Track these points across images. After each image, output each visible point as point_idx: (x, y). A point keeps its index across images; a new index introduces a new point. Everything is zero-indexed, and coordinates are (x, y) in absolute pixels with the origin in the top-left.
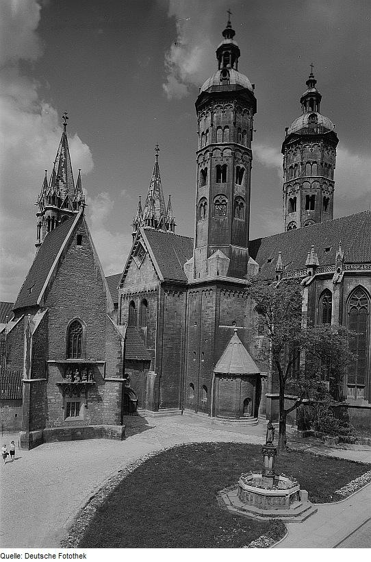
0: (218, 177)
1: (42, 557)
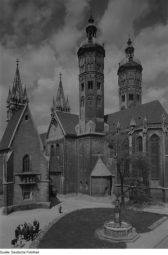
0: (89, 87)
1: (19, 253)
